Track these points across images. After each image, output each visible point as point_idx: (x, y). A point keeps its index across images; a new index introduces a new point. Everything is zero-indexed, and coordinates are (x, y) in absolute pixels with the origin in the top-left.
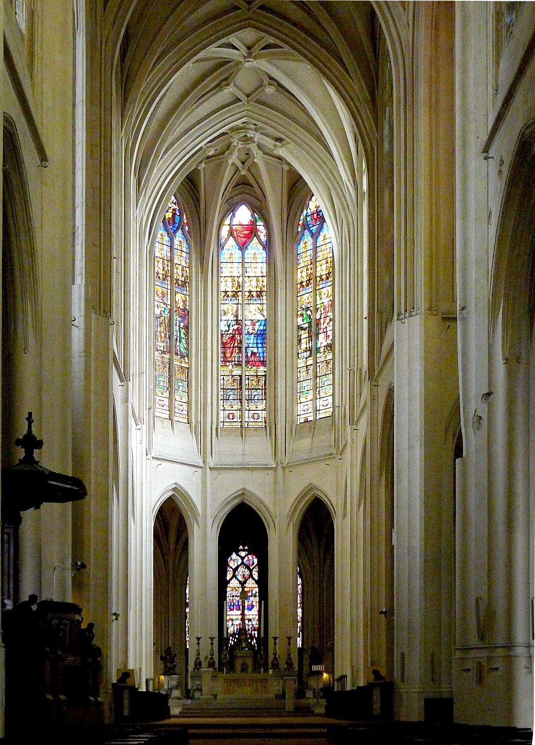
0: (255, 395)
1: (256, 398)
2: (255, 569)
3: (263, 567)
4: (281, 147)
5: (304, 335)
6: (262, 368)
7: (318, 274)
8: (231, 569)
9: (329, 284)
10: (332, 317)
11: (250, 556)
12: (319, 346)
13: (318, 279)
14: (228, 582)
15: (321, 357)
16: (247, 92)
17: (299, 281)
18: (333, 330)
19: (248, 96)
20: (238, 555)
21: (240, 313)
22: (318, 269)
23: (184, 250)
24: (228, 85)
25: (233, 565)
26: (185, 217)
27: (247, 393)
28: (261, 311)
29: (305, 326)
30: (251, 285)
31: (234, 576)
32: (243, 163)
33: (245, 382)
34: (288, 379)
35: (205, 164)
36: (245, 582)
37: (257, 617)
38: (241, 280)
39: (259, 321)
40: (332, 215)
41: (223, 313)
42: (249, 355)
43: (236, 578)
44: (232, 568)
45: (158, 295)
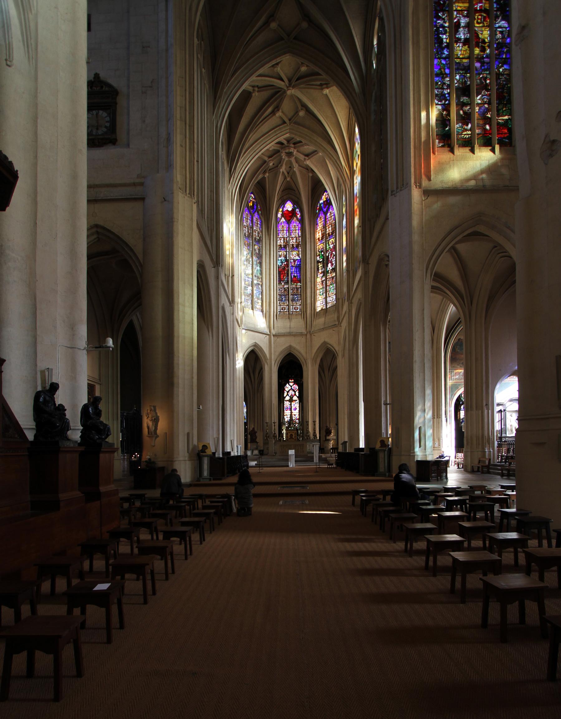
0: (296, 298)
1: (296, 299)
3: (301, 390)
4: (308, 160)
5: (320, 265)
6: (299, 284)
7: (327, 233)
9: (333, 237)
10: (335, 254)
11: (295, 385)
12: (328, 269)
13: (327, 235)
14: (285, 398)
15: (329, 276)
16: (290, 117)
17: (317, 238)
18: (336, 261)
19: (290, 120)
20: (289, 385)
21: (288, 256)
22: (327, 230)
23: (259, 223)
24: (278, 110)
25: (287, 389)
26: (259, 206)
27: (291, 297)
28: (298, 255)
29: (320, 260)
30: (293, 242)
31: (288, 395)
32: (288, 173)
33: (290, 291)
34: (312, 289)
35: (269, 173)
37: (298, 414)
38: (288, 239)
39: (297, 260)
40: (335, 198)
41: (279, 256)
42: (293, 277)
45: (245, 245)
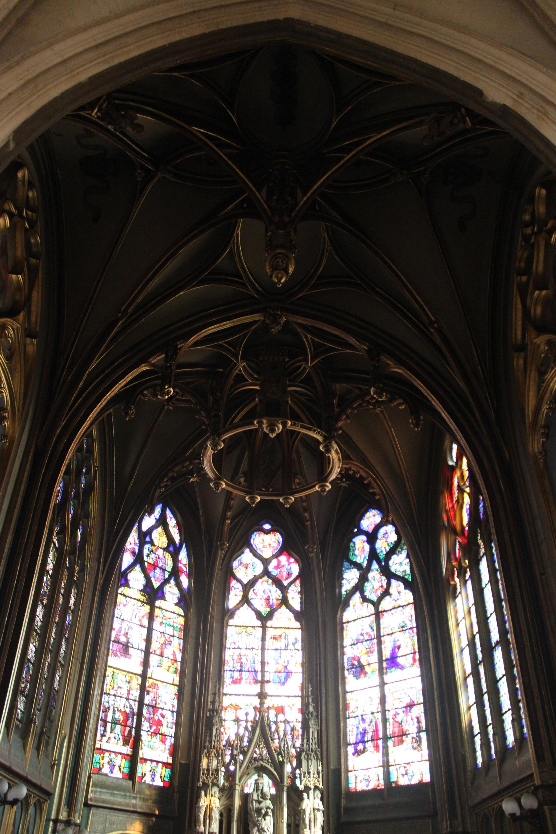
2: (292, 588)
8: (239, 585)
14: (231, 614)
31: (246, 600)
36: (270, 616)
43: (250, 605)
44: (239, 581)
